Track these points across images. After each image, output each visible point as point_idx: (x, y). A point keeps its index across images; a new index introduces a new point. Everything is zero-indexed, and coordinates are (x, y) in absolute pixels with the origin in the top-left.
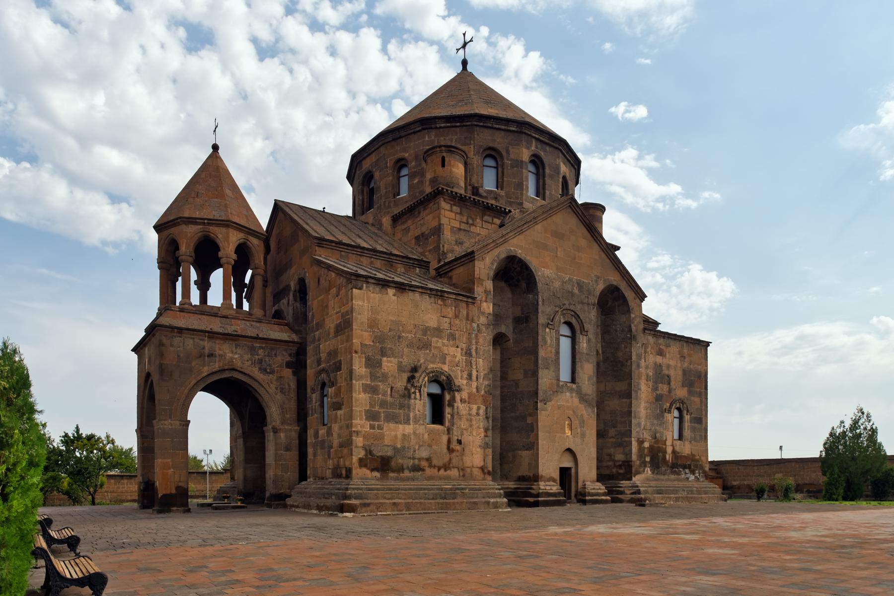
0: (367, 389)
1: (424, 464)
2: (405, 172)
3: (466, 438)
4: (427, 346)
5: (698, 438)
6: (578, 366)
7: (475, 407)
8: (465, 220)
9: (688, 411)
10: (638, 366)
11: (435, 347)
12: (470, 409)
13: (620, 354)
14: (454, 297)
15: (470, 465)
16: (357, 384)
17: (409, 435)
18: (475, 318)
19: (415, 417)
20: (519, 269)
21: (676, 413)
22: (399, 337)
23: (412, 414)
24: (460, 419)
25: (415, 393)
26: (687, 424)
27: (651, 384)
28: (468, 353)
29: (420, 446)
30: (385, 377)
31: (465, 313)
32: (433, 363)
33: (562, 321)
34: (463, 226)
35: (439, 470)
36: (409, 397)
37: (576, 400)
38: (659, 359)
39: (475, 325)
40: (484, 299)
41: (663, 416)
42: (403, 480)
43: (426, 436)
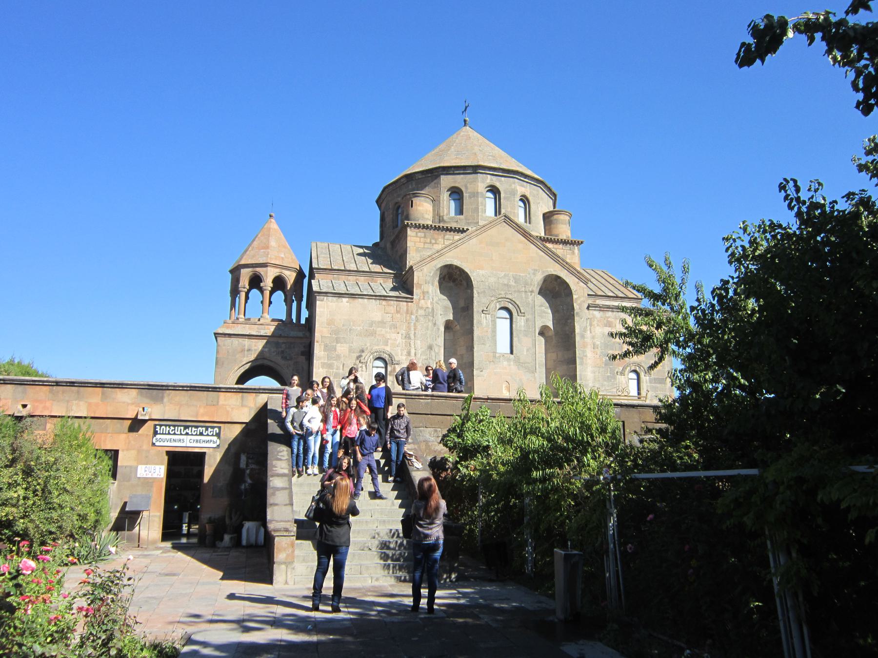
0: (324, 365)
2: (400, 211)
4: (373, 334)
6: (515, 339)
8: (428, 241)
10: (583, 337)
13: (567, 328)
16: (316, 363)
18: (414, 311)
21: (634, 376)
27: (599, 351)
28: (408, 337)
30: (338, 357)
31: (405, 309)
33: (498, 307)
34: (427, 246)
37: (513, 368)
39: (413, 317)
41: (615, 378)
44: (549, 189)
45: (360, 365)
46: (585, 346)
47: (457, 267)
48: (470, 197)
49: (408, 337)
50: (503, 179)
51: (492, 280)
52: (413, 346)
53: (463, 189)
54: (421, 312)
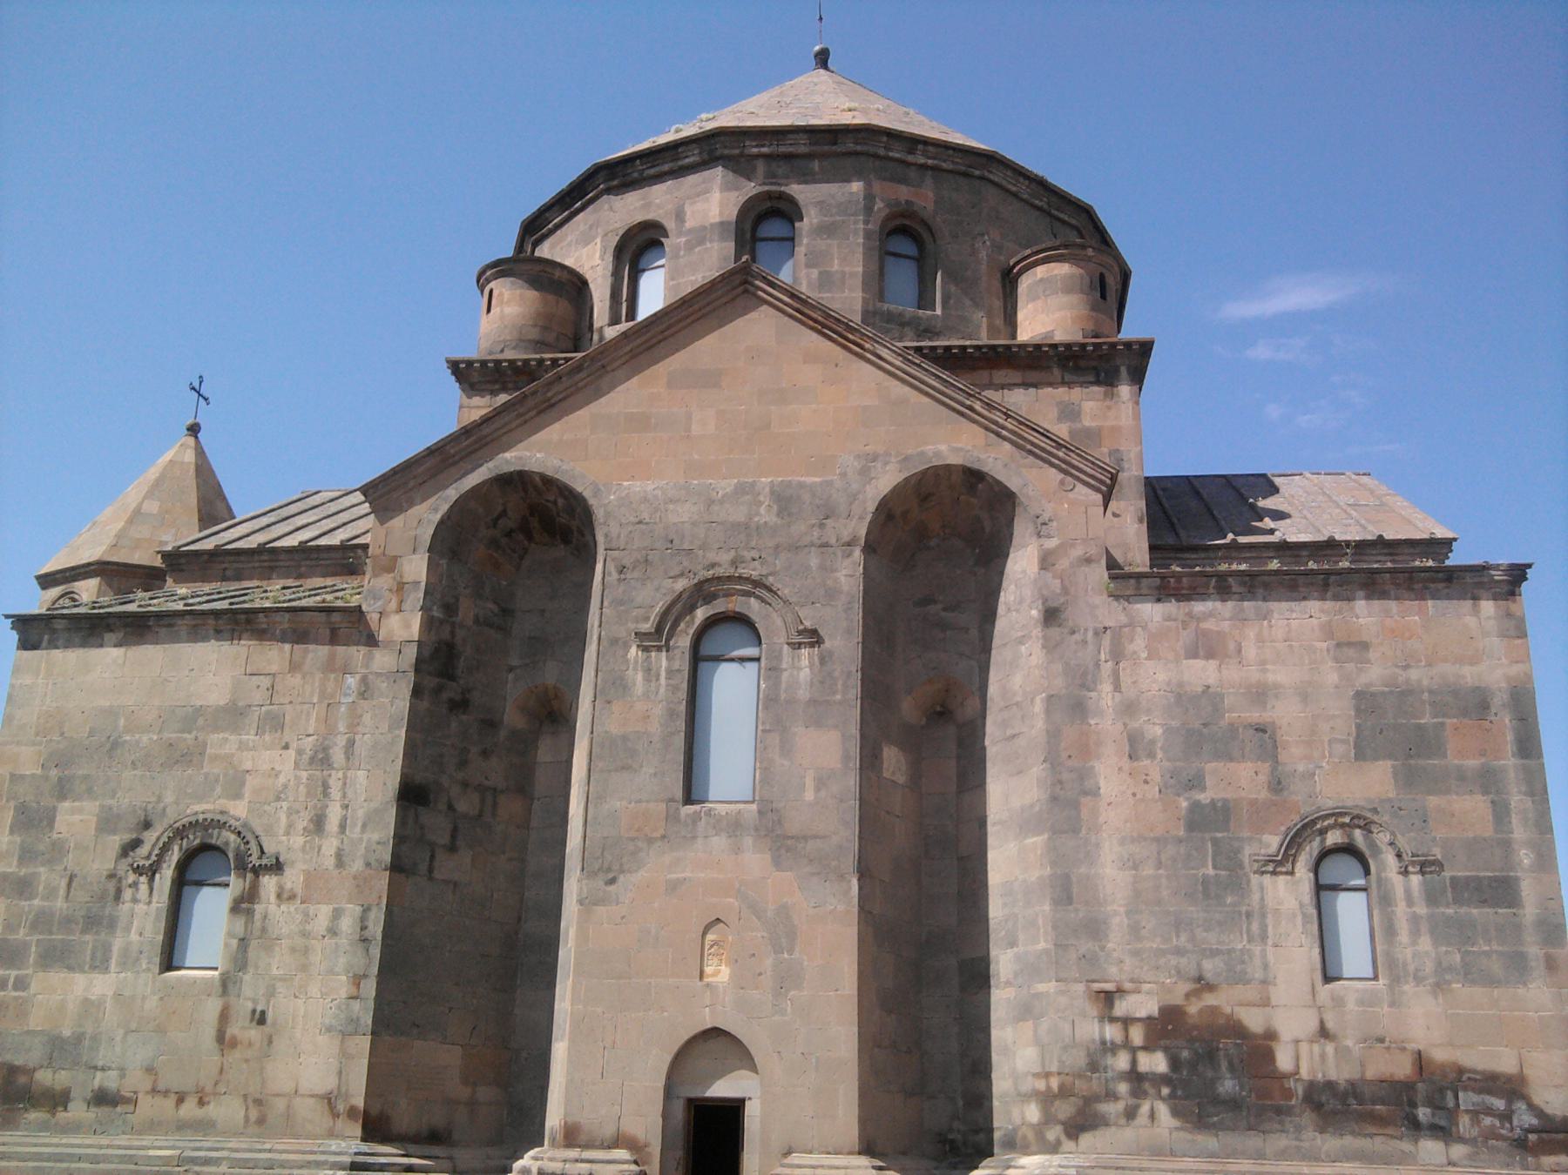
1: (136, 1081)
3: (283, 1007)
5: (1496, 967)
7: (324, 911)
9: (1399, 856)
11: (215, 758)
12: (307, 917)
14: (287, 616)
15: (288, 1087)
17: (99, 1004)
19: (125, 953)
20: (561, 502)
22: (115, 745)
23: (117, 944)
24: (269, 949)
25: (135, 885)
26: (1401, 909)
27: (1155, 769)
28: (321, 759)
29: (128, 1032)
30: (58, 850)
32: (201, 798)
35: (181, 1100)
36: (118, 896)
37: (755, 861)
38: (1201, 673)
39: (351, 681)
40: (393, 605)
42: (66, 1129)
43: (152, 1003)
44: (1042, 183)
45: (132, 877)
46: (1086, 749)
47: (548, 481)
48: (690, 247)
49: (321, 759)
50: (816, 165)
51: (683, 514)
52: (335, 793)
53: (670, 225)
54: (383, 660)
